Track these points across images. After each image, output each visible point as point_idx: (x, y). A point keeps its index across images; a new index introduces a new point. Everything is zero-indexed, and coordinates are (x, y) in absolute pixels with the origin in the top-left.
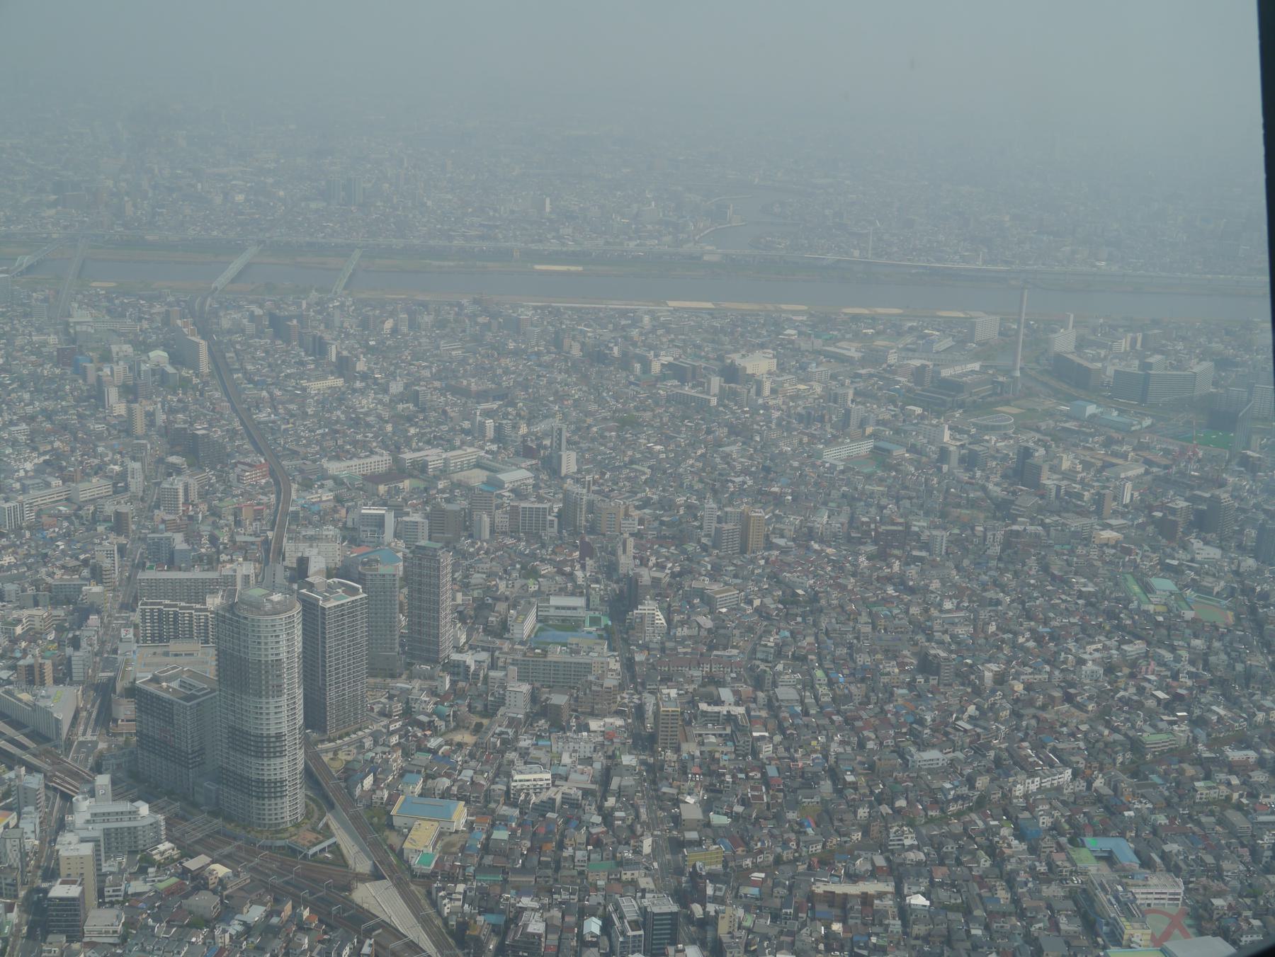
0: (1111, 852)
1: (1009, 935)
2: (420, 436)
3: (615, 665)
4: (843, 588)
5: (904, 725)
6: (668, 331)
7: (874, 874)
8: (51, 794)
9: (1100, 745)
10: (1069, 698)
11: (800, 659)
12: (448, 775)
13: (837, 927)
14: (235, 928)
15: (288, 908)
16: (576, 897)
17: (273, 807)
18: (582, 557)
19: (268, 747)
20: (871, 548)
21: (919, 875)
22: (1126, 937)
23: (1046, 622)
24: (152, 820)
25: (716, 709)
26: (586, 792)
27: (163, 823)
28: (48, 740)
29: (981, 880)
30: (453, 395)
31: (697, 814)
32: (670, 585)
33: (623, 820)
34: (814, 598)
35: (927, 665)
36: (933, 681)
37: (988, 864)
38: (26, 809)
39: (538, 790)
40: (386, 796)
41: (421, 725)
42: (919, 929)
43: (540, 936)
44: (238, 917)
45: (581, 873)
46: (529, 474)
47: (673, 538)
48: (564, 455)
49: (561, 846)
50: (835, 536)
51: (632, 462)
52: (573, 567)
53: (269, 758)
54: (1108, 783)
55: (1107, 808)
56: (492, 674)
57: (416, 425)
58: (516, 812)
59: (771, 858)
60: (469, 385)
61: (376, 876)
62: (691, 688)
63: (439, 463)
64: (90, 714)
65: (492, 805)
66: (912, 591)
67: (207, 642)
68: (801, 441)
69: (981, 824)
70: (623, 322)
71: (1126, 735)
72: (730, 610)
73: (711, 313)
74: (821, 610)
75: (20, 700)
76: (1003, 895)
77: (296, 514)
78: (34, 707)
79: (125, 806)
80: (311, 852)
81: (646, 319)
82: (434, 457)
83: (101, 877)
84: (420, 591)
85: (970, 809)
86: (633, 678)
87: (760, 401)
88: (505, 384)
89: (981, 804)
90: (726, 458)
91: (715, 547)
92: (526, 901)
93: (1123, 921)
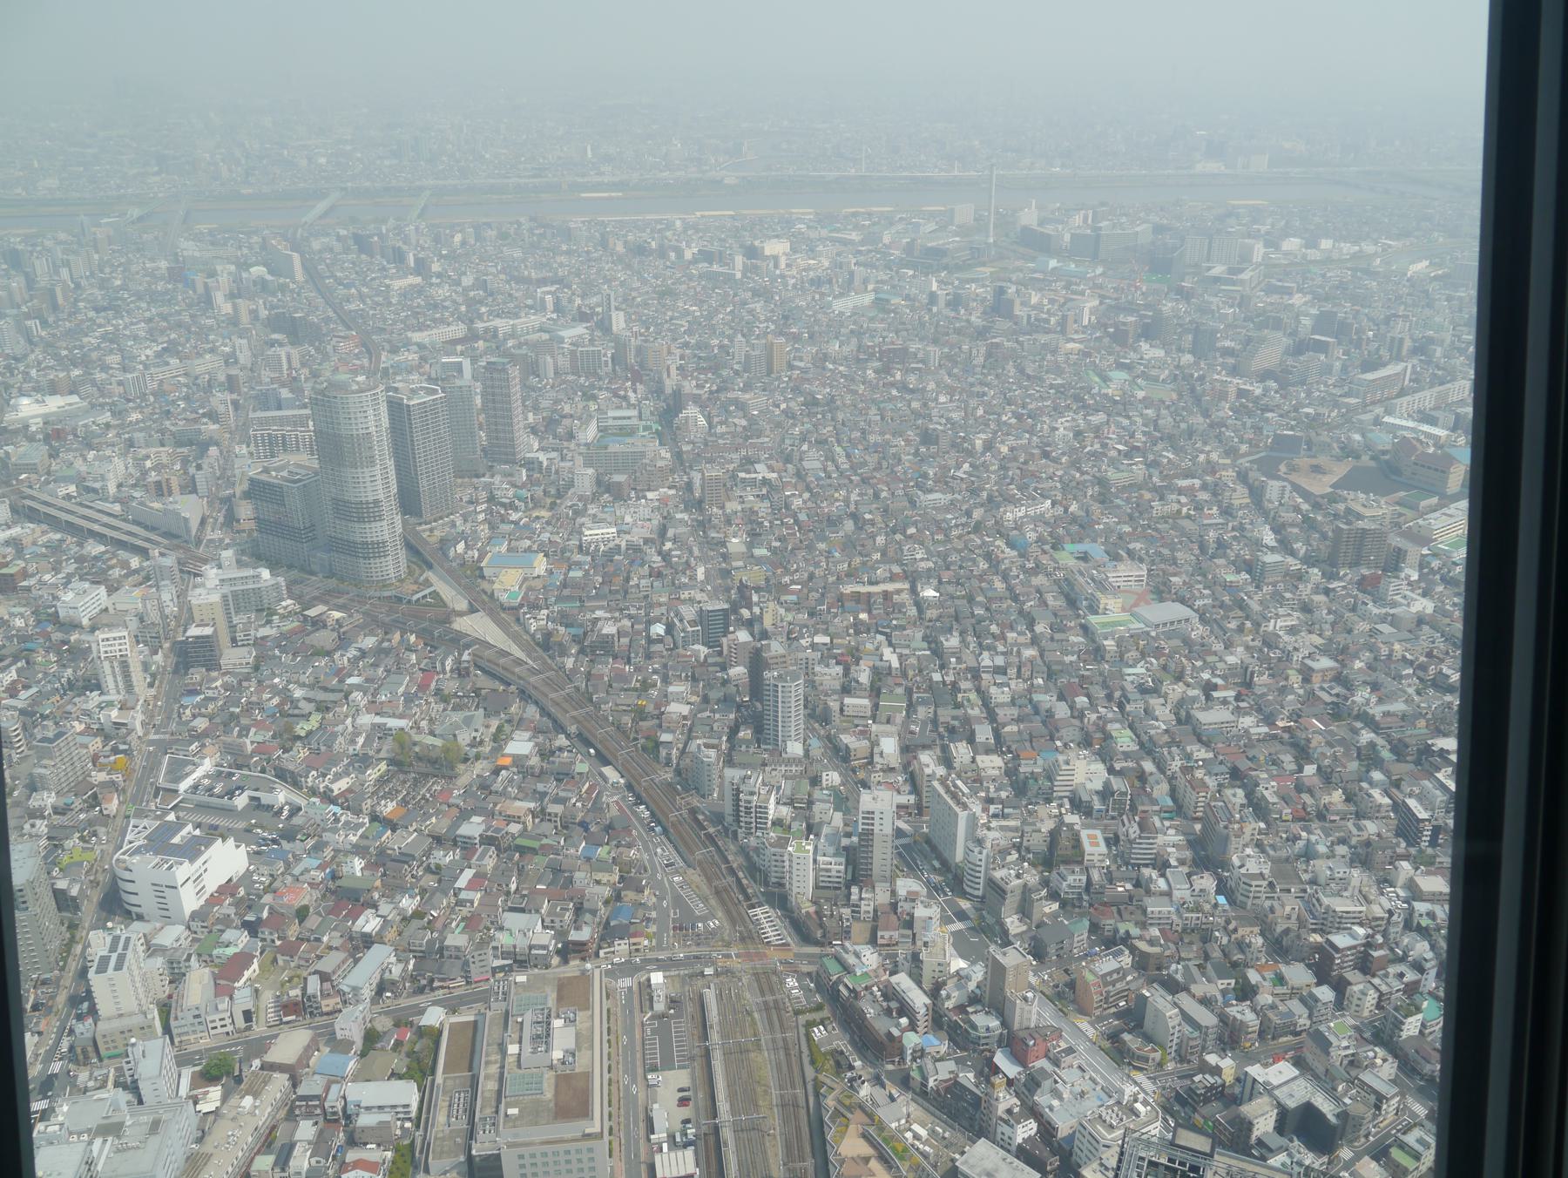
0: (1086, 553)
1: (1007, 612)
2: (490, 313)
3: (665, 453)
4: (855, 392)
5: (911, 479)
6: (697, 231)
7: (893, 578)
8: (186, 576)
9: (1074, 484)
10: (1046, 455)
11: (821, 442)
12: (530, 538)
13: (863, 616)
14: (352, 653)
15: (397, 636)
16: (642, 612)
18: (634, 384)
19: (368, 512)
20: (877, 364)
21: (929, 578)
22: (1102, 606)
23: (1024, 408)
24: (273, 582)
25: (753, 476)
26: (646, 541)
28: (176, 537)
29: (981, 578)
30: (517, 283)
31: (743, 549)
32: (709, 399)
33: (679, 557)
34: (831, 400)
35: (928, 438)
36: (933, 449)
37: (986, 566)
39: (606, 541)
40: (476, 555)
41: (503, 505)
42: (931, 613)
43: (613, 636)
45: (646, 597)
46: (586, 331)
47: (711, 368)
48: (614, 314)
49: (628, 579)
50: (846, 358)
51: (671, 319)
52: (626, 390)
54: (1080, 508)
55: (1081, 526)
56: (562, 464)
57: (487, 305)
58: (589, 558)
59: (806, 575)
60: (530, 273)
61: (472, 610)
62: (731, 467)
63: (508, 329)
65: (568, 554)
66: (912, 391)
68: (813, 298)
69: (979, 542)
70: (659, 227)
71: (1094, 476)
72: (760, 412)
73: (732, 217)
74: (837, 408)
75: (152, 508)
76: (999, 585)
77: (386, 369)
78: (165, 512)
79: (250, 572)
80: (415, 597)
81: (678, 223)
82: (503, 325)
83: (232, 627)
84: (494, 401)
85: (969, 533)
86: (682, 464)
87: (778, 272)
88: (560, 274)
89: (977, 528)
90: (751, 312)
91: (745, 371)
92: (599, 613)
93: (1098, 594)
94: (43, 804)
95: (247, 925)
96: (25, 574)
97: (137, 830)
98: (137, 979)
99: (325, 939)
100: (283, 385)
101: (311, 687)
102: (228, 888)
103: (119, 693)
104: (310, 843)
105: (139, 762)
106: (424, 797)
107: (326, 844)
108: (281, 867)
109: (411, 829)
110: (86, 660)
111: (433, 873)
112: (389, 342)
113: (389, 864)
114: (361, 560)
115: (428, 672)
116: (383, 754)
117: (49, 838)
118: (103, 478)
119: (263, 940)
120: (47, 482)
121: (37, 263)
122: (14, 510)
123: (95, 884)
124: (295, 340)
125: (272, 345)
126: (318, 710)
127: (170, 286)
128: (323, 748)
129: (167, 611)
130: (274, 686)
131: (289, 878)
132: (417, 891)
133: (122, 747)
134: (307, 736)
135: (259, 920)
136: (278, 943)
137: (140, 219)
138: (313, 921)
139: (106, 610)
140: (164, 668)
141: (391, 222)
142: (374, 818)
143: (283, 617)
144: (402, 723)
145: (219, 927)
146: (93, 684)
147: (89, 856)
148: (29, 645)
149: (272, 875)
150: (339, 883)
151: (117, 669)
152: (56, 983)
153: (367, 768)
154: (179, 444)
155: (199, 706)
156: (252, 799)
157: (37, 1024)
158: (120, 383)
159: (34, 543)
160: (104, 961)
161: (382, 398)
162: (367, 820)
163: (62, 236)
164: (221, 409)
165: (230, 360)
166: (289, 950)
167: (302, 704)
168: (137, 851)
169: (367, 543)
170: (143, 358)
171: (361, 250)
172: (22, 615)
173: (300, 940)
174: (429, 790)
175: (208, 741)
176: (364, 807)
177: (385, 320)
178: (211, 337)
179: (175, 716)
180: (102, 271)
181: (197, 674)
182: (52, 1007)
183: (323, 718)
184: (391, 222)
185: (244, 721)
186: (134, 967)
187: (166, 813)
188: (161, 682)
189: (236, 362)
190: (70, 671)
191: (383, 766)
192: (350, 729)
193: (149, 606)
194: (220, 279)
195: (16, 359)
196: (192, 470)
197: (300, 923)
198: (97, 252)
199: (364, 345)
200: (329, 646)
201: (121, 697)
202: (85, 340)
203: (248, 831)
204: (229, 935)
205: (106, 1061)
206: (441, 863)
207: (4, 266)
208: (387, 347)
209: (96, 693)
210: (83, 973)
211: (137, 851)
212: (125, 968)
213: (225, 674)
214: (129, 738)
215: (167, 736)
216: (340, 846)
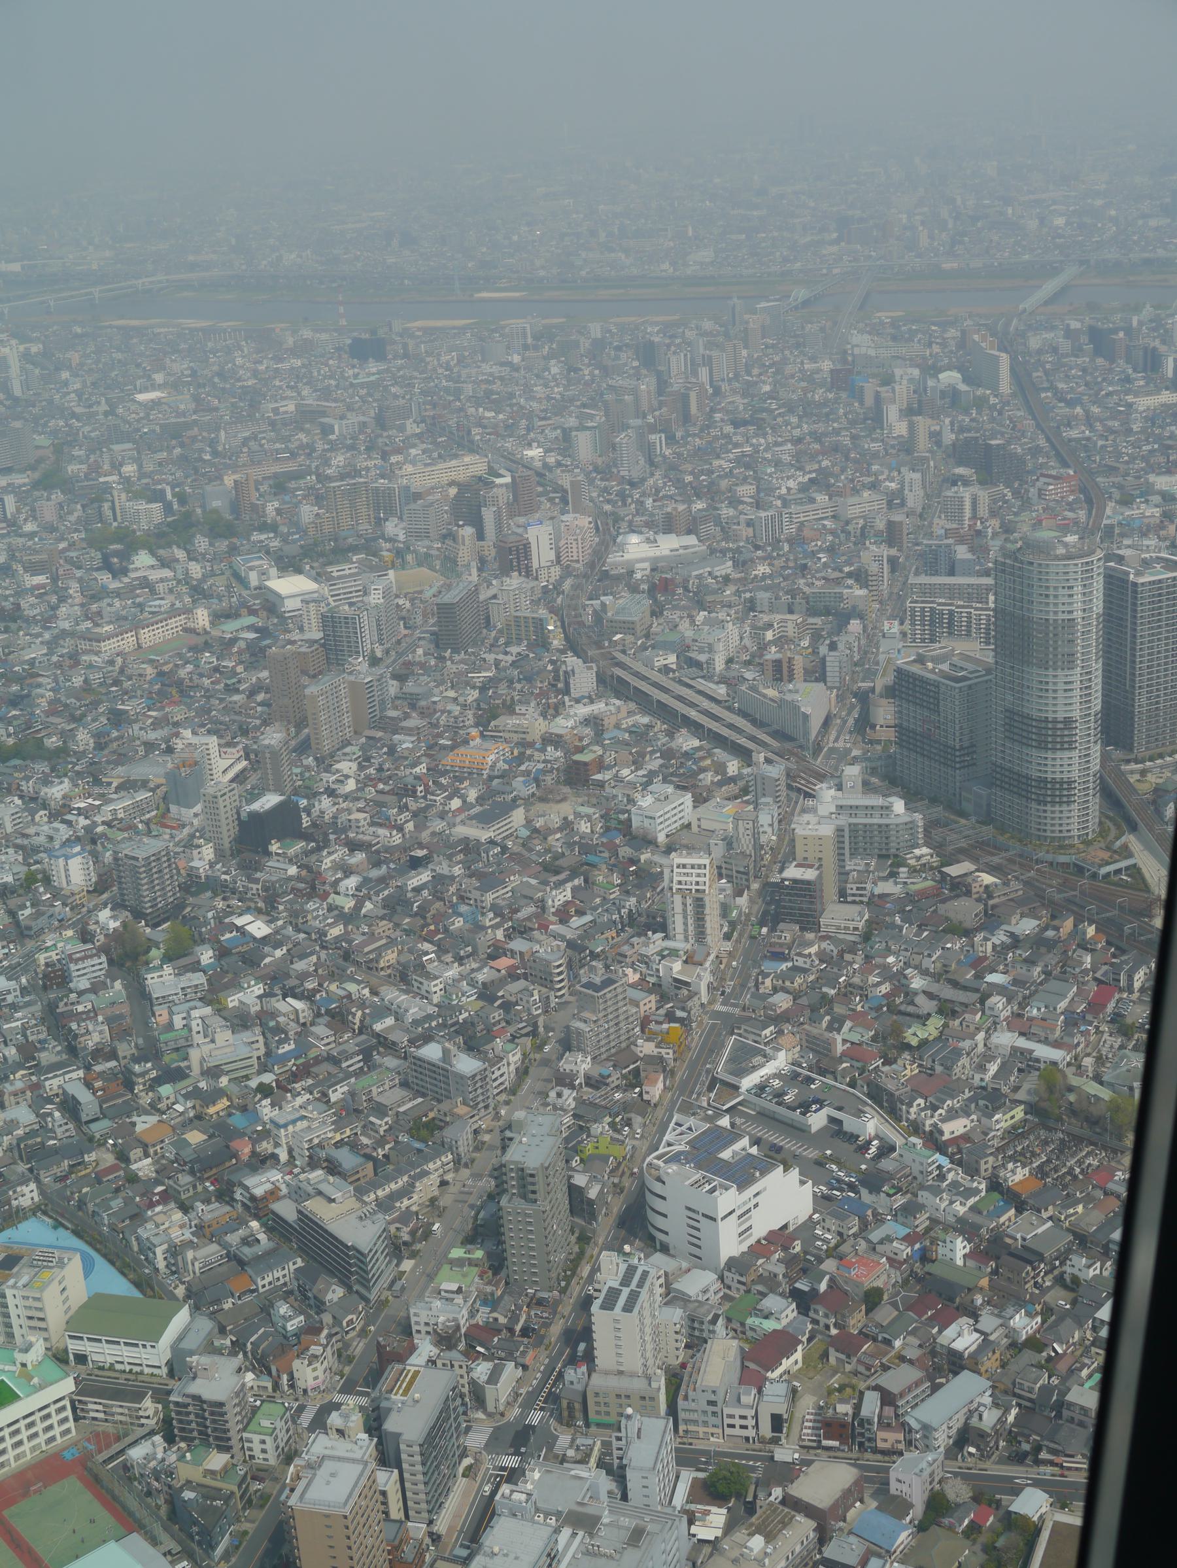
8: (794, 795)
14: (1000, 937)
15: (1068, 924)
17: (1057, 815)
24: (908, 819)
27: (921, 824)
38: (763, 800)
44: (1005, 927)
53: (1054, 750)
64: (845, 722)
67: (987, 643)
75: (765, 696)
78: (781, 703)
79: (878, 801)
80: (1104, 870)
83: (843, 874)
94: (575, 1069)
95: (796, 1295)
96: (600, 765)
97: (679, 1130)
98: (648, 1330)
99: (898, 1343)
100: (961, 541)
101: (936, 977)
102: (780, 1238)
103: (686, 940)
104: (900, 1201)
105: (696, 1039)
106: (1070, 1171)
107: (921, 1207)
108: (854, 1225)
109: (1045, 1215)
110: (654, 889)
111: (1065, 1286)
112: (1120, 487)
113: (1005, 1258)
114: (1034, 805)
115: (1108, 985)
116: (1021, 1095)
117: (575, 1116)
118: (711, 649)
119: (815, 1322)
120: (644, 648)
121: (673, 359)
122: (601, 679)
123: (618, 1189)
124: (986, 478)
125: (954, 483)
126: (940, 1012)
127: (830, 396)
128: (939, 1069)
129: (763, 839)
130: (886, 967)
131: (863, 1243)
132: (1038, 1308)
133: (680, 1014)
134: (919, 1047)
135: (814, 1291)
136: (834, 1332)
137: (806, 303)
138: (885, 1314)
139: (689, 826)
140: (748, 915)
141: (1148, 311)
142: (995, 1185)
143: (913, 871)
144: (1056, 1054)
145: (760, 1288)
146: (658, 923)
147: (617, 1150)
148: (591, 858)
149: (840, 1234)
150: (929, 1268)
151: (689, 908)
152: (551, 1306)
153: (996, 1110)
154: (812, 612)
155: (783, 976)
156: (832, 1120)
157: (524, 1353)
158: (749, 523)
159: (617, 726)
160: (612, 1296)
161: (1098, 569)
162: (983, 1186)
163: (708, 325)
164: (874, 568)
165: (895, 500)
166: (847, 1345)
167: (921, 1000)
168: (675, 1158)
169: (1045, 780)
170: (784, 491)
171: (1097, 352)
172: (589, 818)
173: (865, 1336)
174: (1080, 1163)
175: (787, 1028)
176: (983, 1167)
177: (1119, 455)
178: (875, 468)
179: (751, 984)
180: (749, 373)
181: (787, 932)
182: (543, 1337)
183: (945, 1026)
184: (1148, 311)
185: (839, 1009)
186: (646, 1313)
187: (719, 1114)
188: (741, 935)
189: (903, 504)
190: (633, 900)
191: (1019, 1113)
192: (981, 1048)
193: (741, 830)
194: (897, 387)
195: (632, 484)
196: (823, 650)
197: (867, 1312)
198: (746, 347)
199: (1083, 490)
200: (969, 922)
201: (689, 947)
202: (716, 463)
203: (820, 1163)
204: (772, 1302)
205: (593, 1429)
206: (1081, 1275)
207: (635, 364)
208: (1117, 495)
209: (660, 935)
210: (586, 1303)
211: (675, 1158)
212: (636, 1310)
213: (826, 938)
214: (690, 1004)
215: (737, 1011)
216: (940, 1216)
